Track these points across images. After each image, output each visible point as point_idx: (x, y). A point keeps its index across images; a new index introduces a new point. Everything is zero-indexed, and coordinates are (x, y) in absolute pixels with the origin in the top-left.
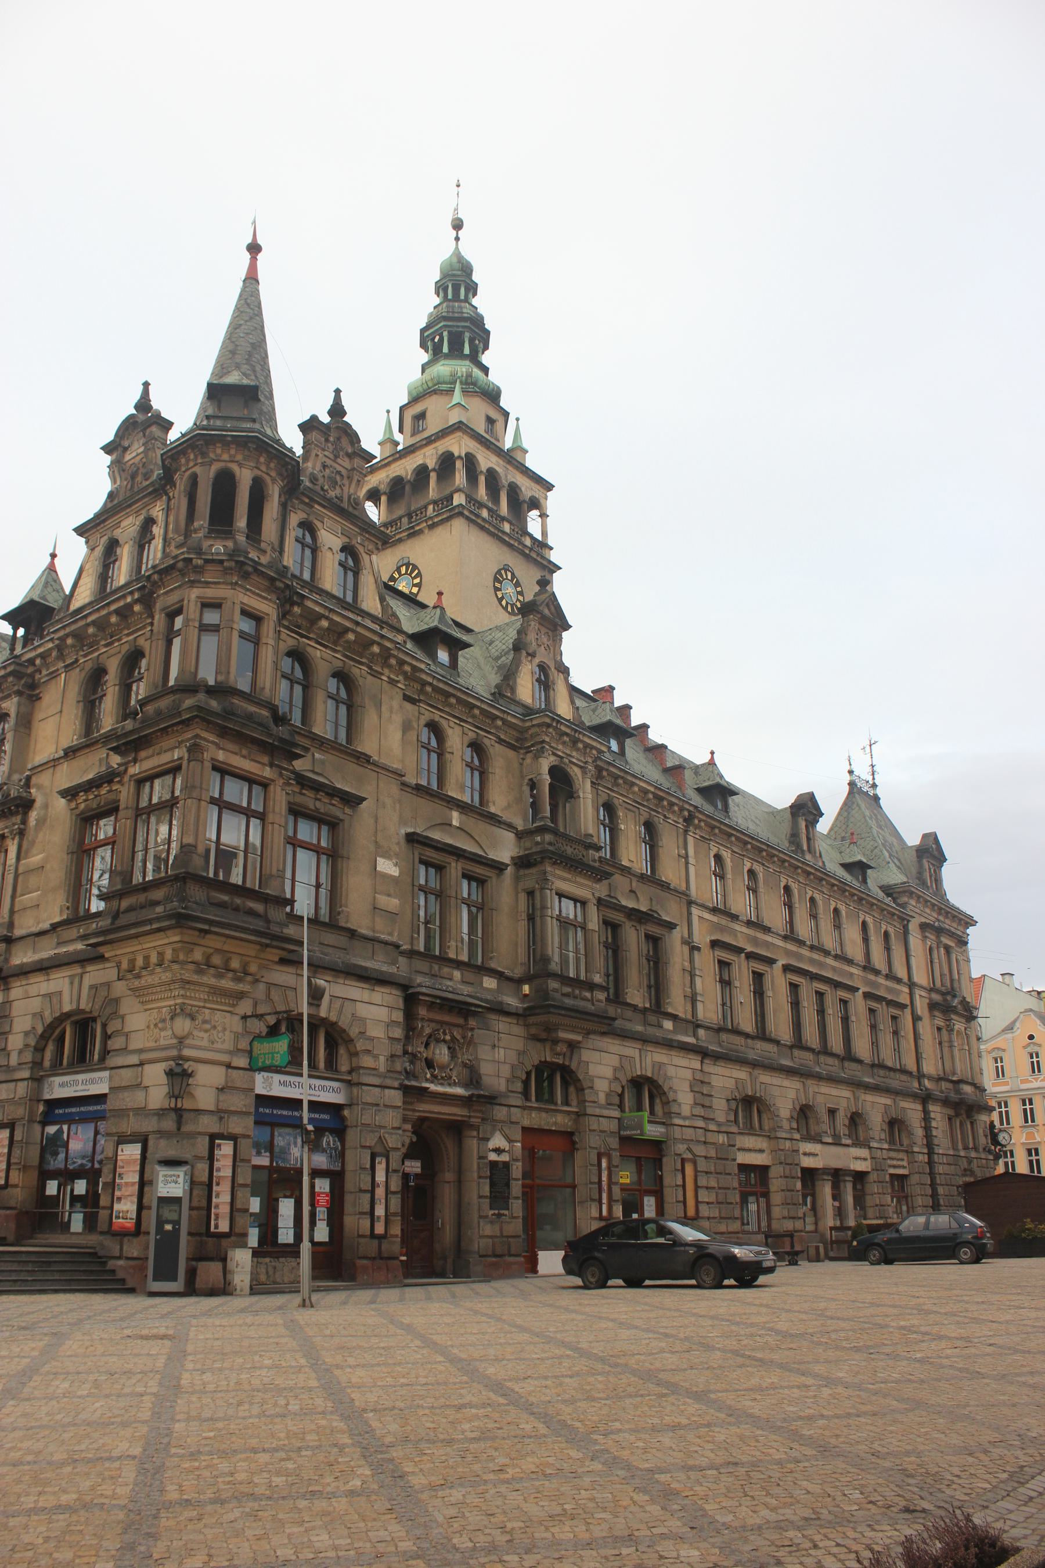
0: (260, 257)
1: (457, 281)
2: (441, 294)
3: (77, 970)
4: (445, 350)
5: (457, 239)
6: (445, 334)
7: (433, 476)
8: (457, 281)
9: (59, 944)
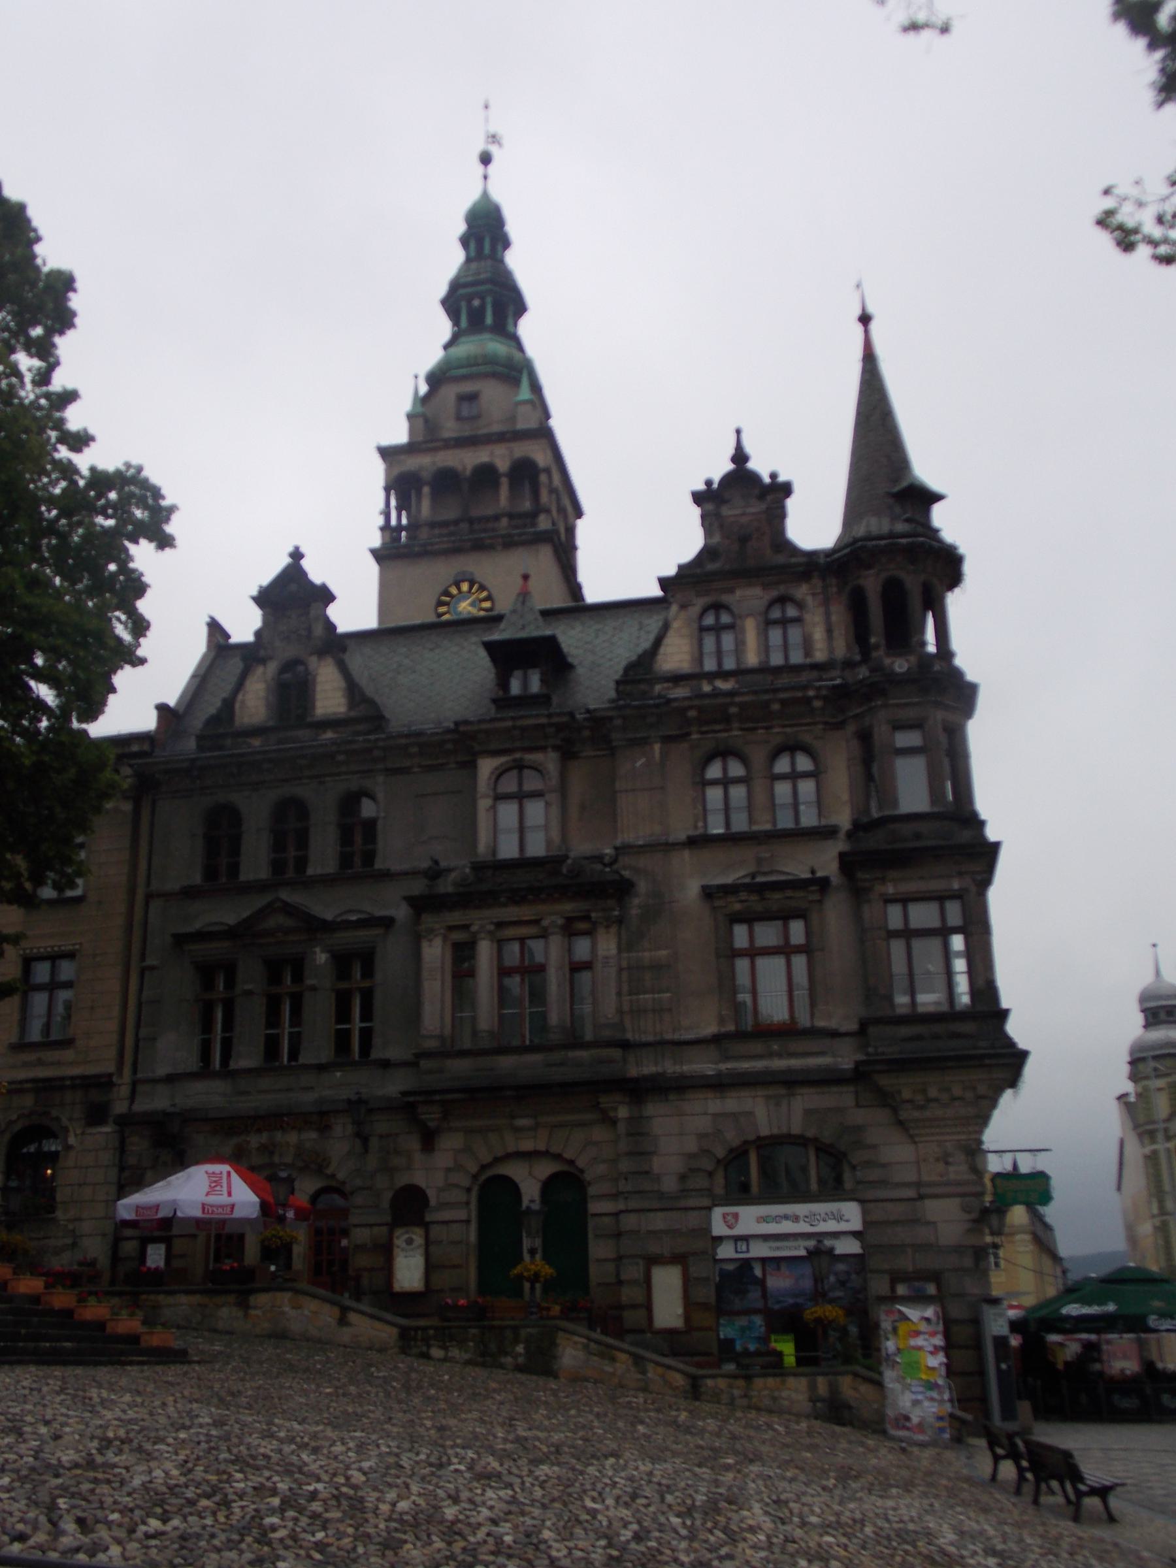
0: (873, 326)
1: (486, 231)
2: (472, 245)
3: (783, 1091)
4: (489, 320)
5: (485, 177)
6: (489, 300)
7: (504, 481)
8: (486, 231)
9: (727, 1058)
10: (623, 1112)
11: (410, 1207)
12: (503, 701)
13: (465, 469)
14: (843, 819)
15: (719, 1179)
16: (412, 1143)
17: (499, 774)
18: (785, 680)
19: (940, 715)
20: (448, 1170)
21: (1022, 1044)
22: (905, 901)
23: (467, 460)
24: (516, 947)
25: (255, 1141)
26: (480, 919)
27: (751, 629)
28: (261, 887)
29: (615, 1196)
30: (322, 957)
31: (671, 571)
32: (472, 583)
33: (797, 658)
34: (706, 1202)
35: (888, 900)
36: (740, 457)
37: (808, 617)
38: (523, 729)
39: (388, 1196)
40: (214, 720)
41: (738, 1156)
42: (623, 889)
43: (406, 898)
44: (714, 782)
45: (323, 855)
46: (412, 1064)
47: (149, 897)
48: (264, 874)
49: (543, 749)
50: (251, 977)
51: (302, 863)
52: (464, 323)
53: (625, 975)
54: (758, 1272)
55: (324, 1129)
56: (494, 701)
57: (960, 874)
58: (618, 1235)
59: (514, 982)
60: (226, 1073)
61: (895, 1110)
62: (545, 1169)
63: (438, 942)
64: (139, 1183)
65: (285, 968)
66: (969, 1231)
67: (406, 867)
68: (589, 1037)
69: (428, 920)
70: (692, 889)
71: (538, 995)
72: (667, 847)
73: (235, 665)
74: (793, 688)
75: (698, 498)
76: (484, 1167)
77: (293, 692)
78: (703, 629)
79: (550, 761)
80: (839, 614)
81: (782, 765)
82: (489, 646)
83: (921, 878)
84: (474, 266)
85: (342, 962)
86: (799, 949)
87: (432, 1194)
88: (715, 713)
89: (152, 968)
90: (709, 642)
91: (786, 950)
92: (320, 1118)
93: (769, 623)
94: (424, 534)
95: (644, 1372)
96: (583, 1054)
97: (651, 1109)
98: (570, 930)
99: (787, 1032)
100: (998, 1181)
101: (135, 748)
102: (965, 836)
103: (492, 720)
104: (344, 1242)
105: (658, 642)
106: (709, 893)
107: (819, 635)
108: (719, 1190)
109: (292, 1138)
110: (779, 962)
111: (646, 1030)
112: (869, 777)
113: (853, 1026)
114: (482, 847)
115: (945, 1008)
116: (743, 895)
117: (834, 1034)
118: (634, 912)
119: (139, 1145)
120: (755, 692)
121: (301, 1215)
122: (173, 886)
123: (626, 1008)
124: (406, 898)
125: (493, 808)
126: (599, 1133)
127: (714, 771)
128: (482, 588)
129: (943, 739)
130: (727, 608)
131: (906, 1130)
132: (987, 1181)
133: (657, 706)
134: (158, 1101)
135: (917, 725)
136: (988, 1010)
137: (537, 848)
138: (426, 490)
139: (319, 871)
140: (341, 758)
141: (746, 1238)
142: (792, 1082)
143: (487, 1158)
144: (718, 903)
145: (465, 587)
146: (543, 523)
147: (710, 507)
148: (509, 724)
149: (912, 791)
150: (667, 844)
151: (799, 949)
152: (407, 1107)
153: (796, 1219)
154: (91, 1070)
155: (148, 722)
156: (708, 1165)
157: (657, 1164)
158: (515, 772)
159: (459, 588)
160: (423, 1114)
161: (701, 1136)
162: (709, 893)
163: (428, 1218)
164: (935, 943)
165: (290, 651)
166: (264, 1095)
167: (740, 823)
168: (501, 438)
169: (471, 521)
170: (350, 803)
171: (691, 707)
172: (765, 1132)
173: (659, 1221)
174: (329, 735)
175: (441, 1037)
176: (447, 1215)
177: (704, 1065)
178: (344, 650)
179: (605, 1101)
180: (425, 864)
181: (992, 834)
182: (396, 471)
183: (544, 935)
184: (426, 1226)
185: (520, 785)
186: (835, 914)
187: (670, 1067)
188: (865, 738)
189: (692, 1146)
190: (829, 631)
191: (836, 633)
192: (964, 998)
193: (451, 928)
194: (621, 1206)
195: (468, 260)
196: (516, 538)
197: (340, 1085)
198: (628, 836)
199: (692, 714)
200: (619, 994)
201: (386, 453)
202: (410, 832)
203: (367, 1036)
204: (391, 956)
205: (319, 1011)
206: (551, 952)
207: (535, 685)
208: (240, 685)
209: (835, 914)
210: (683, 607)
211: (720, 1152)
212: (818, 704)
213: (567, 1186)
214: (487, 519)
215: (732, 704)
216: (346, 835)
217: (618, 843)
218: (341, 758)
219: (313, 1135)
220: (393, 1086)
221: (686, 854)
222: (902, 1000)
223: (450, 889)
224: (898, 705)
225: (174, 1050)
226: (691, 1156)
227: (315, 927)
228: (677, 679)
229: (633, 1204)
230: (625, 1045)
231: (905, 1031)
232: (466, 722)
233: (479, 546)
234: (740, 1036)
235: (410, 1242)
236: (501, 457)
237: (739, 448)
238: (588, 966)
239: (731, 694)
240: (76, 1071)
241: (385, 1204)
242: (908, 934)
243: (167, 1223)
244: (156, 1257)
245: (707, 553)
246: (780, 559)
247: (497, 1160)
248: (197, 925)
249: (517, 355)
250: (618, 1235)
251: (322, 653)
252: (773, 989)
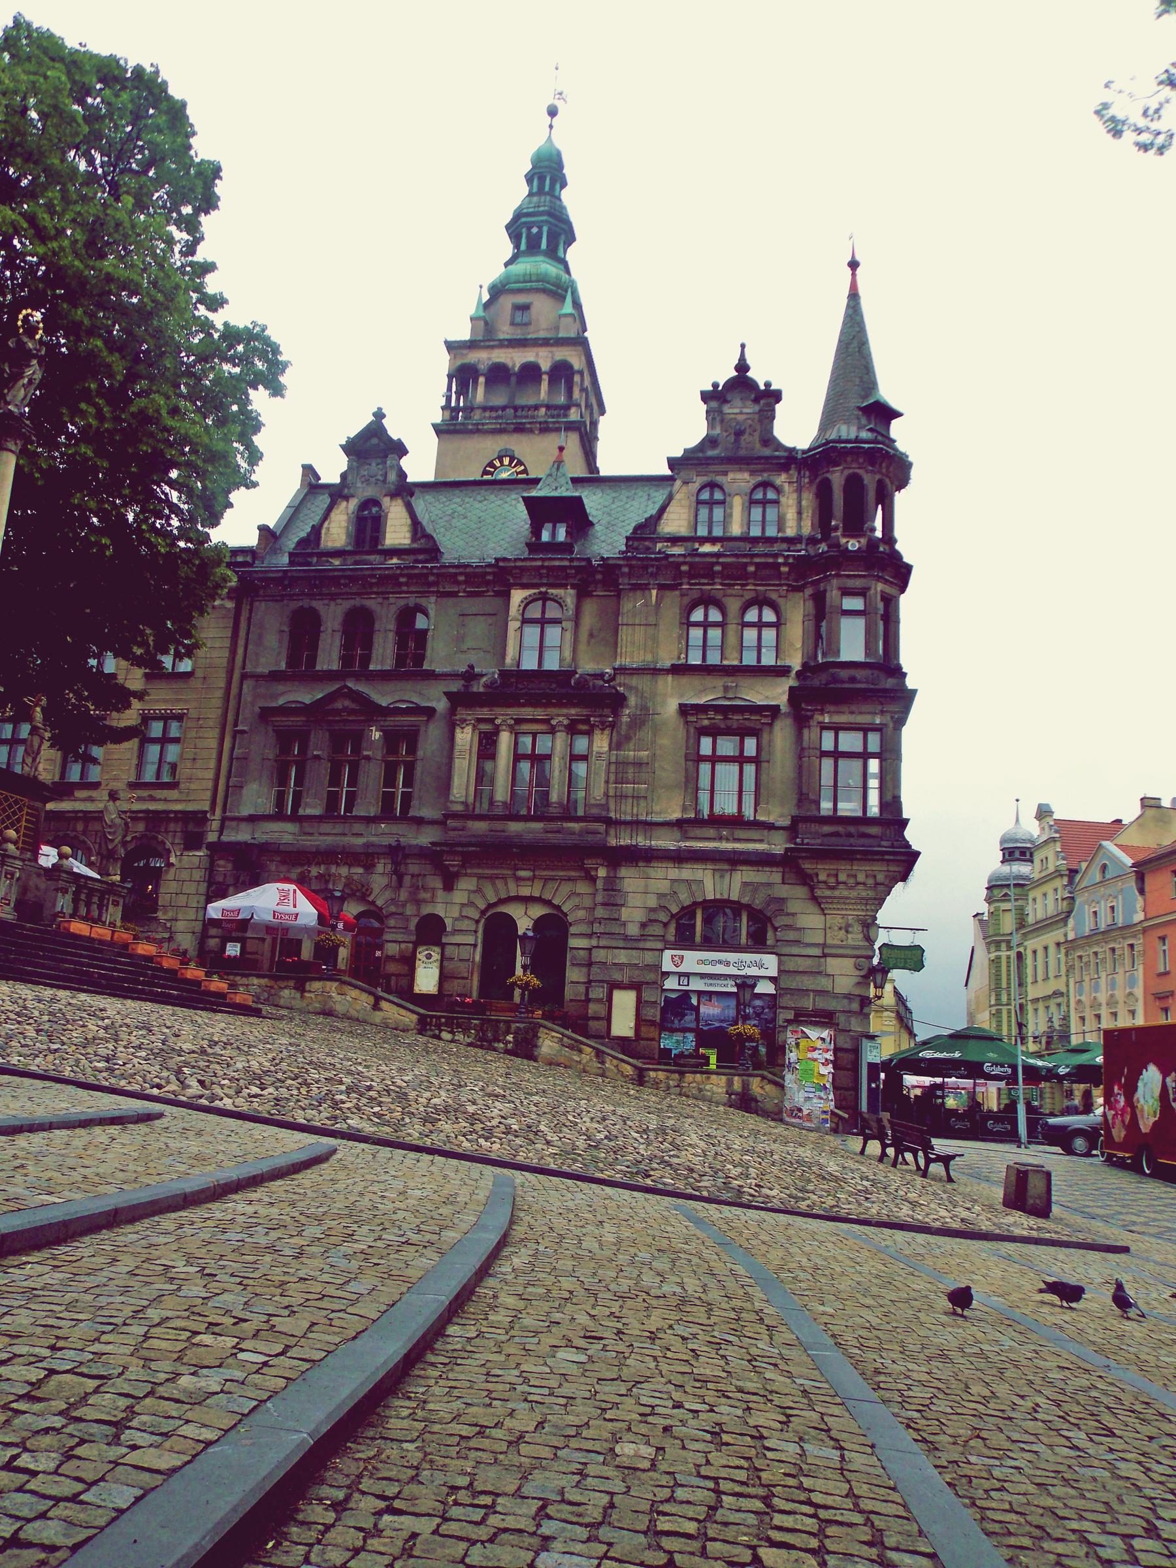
0: (859, 271)
1: (547, 174)
3: (726, 867)
4: (544, 245)
5: (551, 127)
6: (545, 229)
7: (545, 377)
8: (547, 174)
10: (602, 872)
11: (431, 931)
12: (535, 546)
14: (795, 662)
15: (672, 929)
16: (437, 883)
17: (527, 603)
18: (760, 548)
19: (880, 586)
20: (463, 905)
21: (915, 847)
22: (837, 729)
23: (516, 359)
24: (528, 740)
25: (314, 871)
26: (504, 715)
27: (737, 504)
28: (329, 676)
29: (589, 936)
30: (376, 735)
31: (679, 453)
32: (512, 459)
33: (771, 532)
34: (660, 945)
35: (824, 727)
36: (742, 367)
37: (783, 500)
38: (548, 568)
39: (414, 921)
40: (302, 543)
41: (688, 912)
42: (619, 701)
43: (446, 694)
44: (696, 624)
45: (383, 654)
46: (440, 823)
47: (244, 676)
48: (335, 666)
49: (564, 586)
50: (319, 745)
51: (366, 659)
52: (523, 247)
53: (613, 768)
54: (694, 1001)
55: (369, 868)
56: (528, 545)
57: (882, 712)
58: (590, 964)
59: (525, 766)
60: (294, 818)
61: (812, 889)
62: (538, 911)
63: (469, 729)
64: (224, 895)
65: (347, 743)
66: (858, 983)
67: (447, 669)
68: (580, 813)
69: (462, 713)
70: (672, 706)
71: (543, 781)
72: (655, 672)
73: (324, 500)
74: (766, 555)
75: (705, 397)
76: (490, 906)
77: (369, 525)
78: (699, 502)
79: (568, 596)
80: (808, 499)
81: (752, 616)
82: (528, 501)
83: (852, 713)
84: (535, 199)
85: (392, 739)
86: (750, 760)
87: (448, 922)
88: (703, 569)
89: (243, 732)
90: (704, 512)
91: (740, 759)
92: (365, 858)
93: (753, 502)
94: (477, 415)
95: (603, 1063)
96: (575, 826)
97: (623, 872)
98: (572, 729)
99: (736, 822)
100: (884, 950)
101: (240, 559)
102: (890, 683)
103: (525, 560)
104: (378, 954)
105: (662, 510)
106: (684, 710)
107: (791, 515)
108: (671, 937)
109: (344, 871)
110: (735, 768)
111: (627, 811)
112: (818, 636)
113: (786, 822)
114: (508, 660)
115: (860, 814)
116: (711, 714)
117: (770, 827)
118: (625, 719)
119: (224, 866)
120: (736, 556)
121: (347, 927)
122: (263, 669)
123: (611, 793)
124: (446, 694)
125: (521, 628)
126: (583, 888)
127: (698, 615)
128: (520, 463)
129: (881, 605)
130: (721, 488)
131: (819, 904)
132: (876, 946)
133: (656, 559)
134: (241, 835)
135: (862, 593)
136: (893, 819)
137: (552, 663)
138: (482, 380)
139: (379, 668)
140: (403, 580)
141: (687, 975)
142: (735, 860)
143: (493, 900)
144: (691, 719)
145: (506, 461)
146: (574, 415)
147: (714, 404)
148: (539, 563)
149: (852, 643)
150: (655, 669)
151: (750, 760)
152: (432, 856)
153: (728, 964)
154: (190, 807)
155: (251, 539)
156: (663, 917)
157: (625, 914)
158: (540, 603)
160: (447, 863)
161: (661, 896)
162: (684, 710)
163: (444, 940)
164: (857, 764)
165: (369, 492)
166: (325, 837)
167: (714, 658)
168: (545, 343)
169: (516, 409)
170: (406, 617)
171: (684, 563)
172: (710, 896)
173: (622, 957)
174: (395, 561)
175: (465, 804)
176: (457, 939)
177: (666, 841)
178: (412, 495)
179: (589, 863)
180: (463, 669)
181: (910, 683)
182: (459, 363)
183: (552, 731)
184: (443, 946)
185: (543, 612)
186: (781, 736)
187: (641, 841)
188: (819, 599)
189: (652, 902)
190: (800, 513)
191: (804, 515)
192: (874, 810)
193: (479, 720)
194: (594, 942)
195: (530, 194)
197: (384, 834)
198: (624, 661)
199: (684, 568)
200: (607, 782)
201: (451, 346)
202: (453, 640)
203: (407, 798)
204: (431, 738)
205: (372, 776)
206: (556, 745)
207: (561, 535)
208: (326, 516)
209: (781, 736)
210: (686, 483)
211: (675, 909)
212: (784, 569)
213: (553, 928)
214: (529, 408)
215: (718, 563)
216: (401, 644)
217: (617, 664)
218: (403, 580)
219: (360, 870)
220: (425, 838)
221: (670, 678)
222: (826, 806)
223: (481, 690)
224: (849, 576)
225: (256, 797)
226: (652, 910)
227: (373, 712)
228: (675, 540)
229: (603, 943)
230: (609, 822)
231: (827, 829)
232: (505, 559)
233: (520, 429)
234: (698, 822)
235: (429, 957)
236: (544, 359)
237: (742, 358)
238: (584, 758)
239: (717, 555)
240: (179, 807)
241: (412, 925)
242: (836, 755)
243: (244, 924)
244: (233, 949)
245: (709, 441)
246: (767, 452)
247: (501, 902)
248: (281, 701)
249: (565, 276)
250: (590, 964)
251: (393, 495)
252: (726, 791)
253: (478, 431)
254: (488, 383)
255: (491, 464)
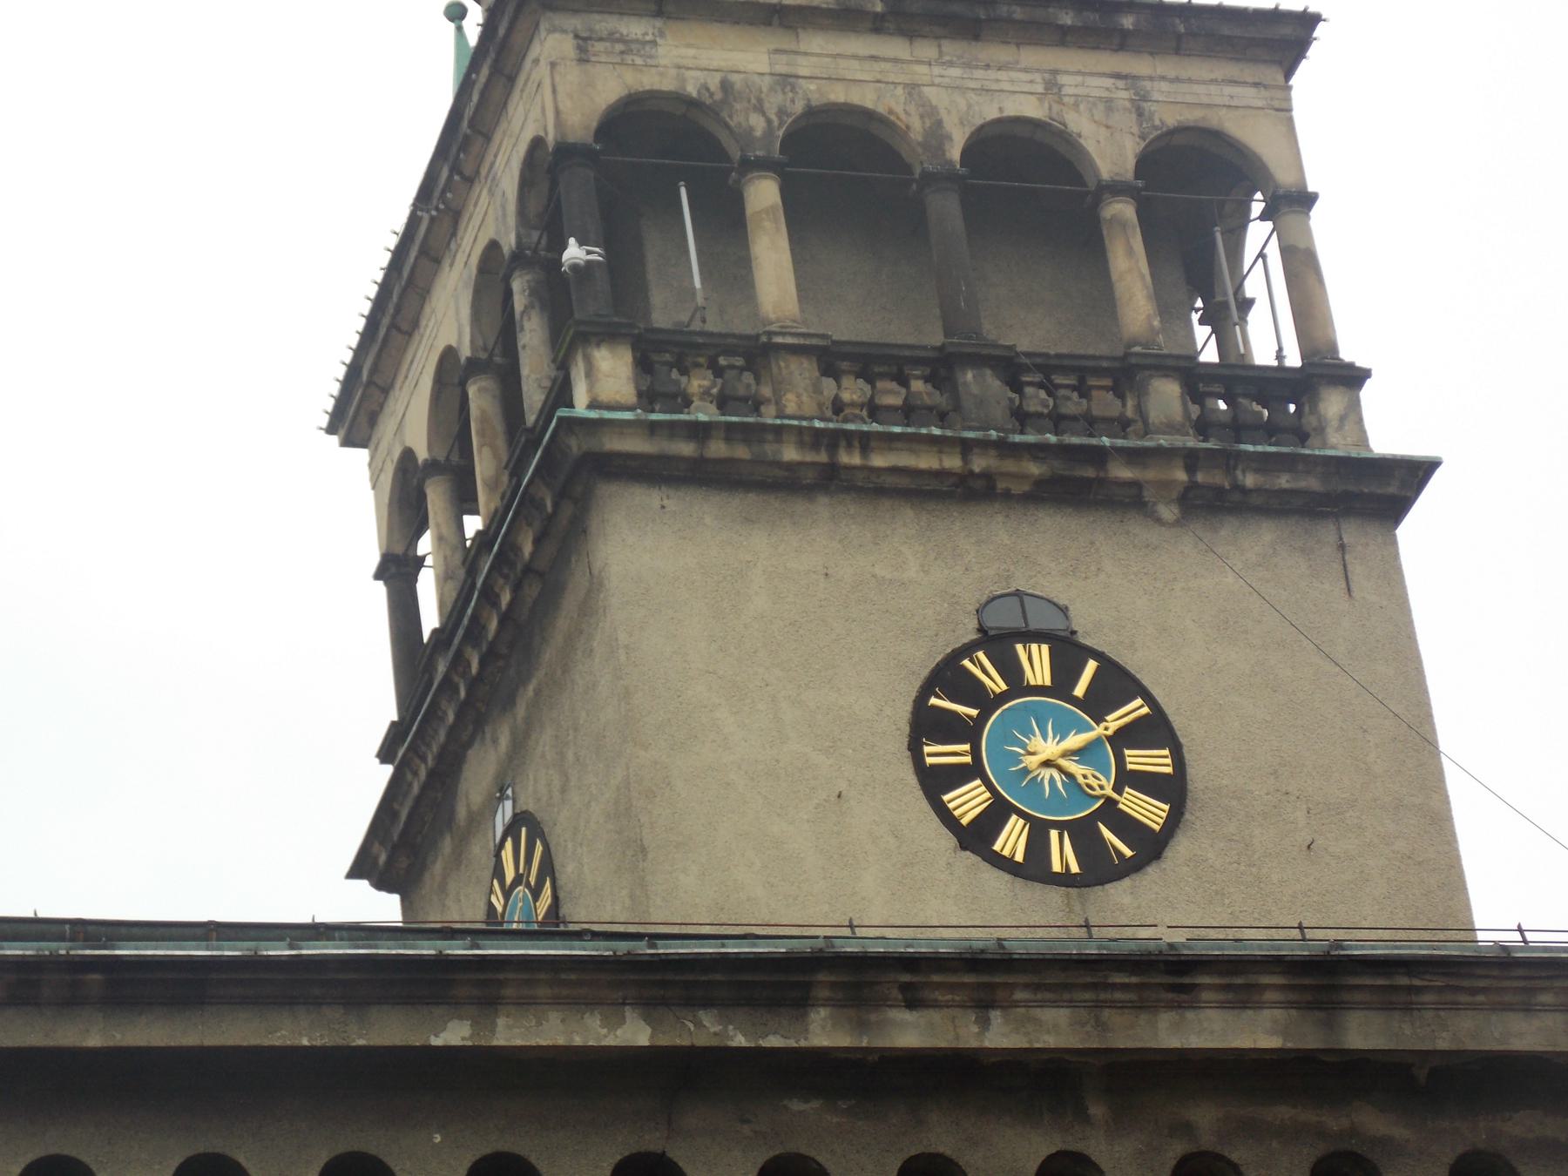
13: (937, 136)
128: (1116, 684)
138: (763, 194)
159: (1011, 670)
196: (1250, 480)
233: (1079, 485)
253: (829, 481)
254: (801, 216)
255: (948, 675)
